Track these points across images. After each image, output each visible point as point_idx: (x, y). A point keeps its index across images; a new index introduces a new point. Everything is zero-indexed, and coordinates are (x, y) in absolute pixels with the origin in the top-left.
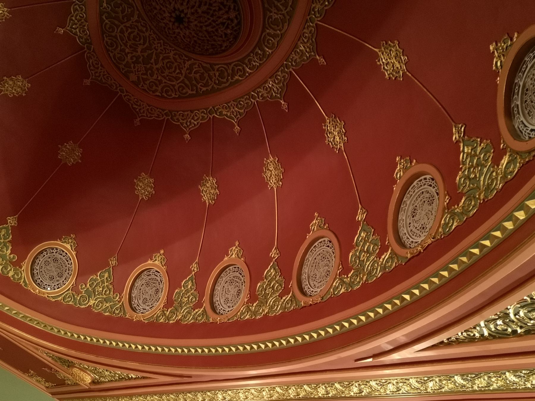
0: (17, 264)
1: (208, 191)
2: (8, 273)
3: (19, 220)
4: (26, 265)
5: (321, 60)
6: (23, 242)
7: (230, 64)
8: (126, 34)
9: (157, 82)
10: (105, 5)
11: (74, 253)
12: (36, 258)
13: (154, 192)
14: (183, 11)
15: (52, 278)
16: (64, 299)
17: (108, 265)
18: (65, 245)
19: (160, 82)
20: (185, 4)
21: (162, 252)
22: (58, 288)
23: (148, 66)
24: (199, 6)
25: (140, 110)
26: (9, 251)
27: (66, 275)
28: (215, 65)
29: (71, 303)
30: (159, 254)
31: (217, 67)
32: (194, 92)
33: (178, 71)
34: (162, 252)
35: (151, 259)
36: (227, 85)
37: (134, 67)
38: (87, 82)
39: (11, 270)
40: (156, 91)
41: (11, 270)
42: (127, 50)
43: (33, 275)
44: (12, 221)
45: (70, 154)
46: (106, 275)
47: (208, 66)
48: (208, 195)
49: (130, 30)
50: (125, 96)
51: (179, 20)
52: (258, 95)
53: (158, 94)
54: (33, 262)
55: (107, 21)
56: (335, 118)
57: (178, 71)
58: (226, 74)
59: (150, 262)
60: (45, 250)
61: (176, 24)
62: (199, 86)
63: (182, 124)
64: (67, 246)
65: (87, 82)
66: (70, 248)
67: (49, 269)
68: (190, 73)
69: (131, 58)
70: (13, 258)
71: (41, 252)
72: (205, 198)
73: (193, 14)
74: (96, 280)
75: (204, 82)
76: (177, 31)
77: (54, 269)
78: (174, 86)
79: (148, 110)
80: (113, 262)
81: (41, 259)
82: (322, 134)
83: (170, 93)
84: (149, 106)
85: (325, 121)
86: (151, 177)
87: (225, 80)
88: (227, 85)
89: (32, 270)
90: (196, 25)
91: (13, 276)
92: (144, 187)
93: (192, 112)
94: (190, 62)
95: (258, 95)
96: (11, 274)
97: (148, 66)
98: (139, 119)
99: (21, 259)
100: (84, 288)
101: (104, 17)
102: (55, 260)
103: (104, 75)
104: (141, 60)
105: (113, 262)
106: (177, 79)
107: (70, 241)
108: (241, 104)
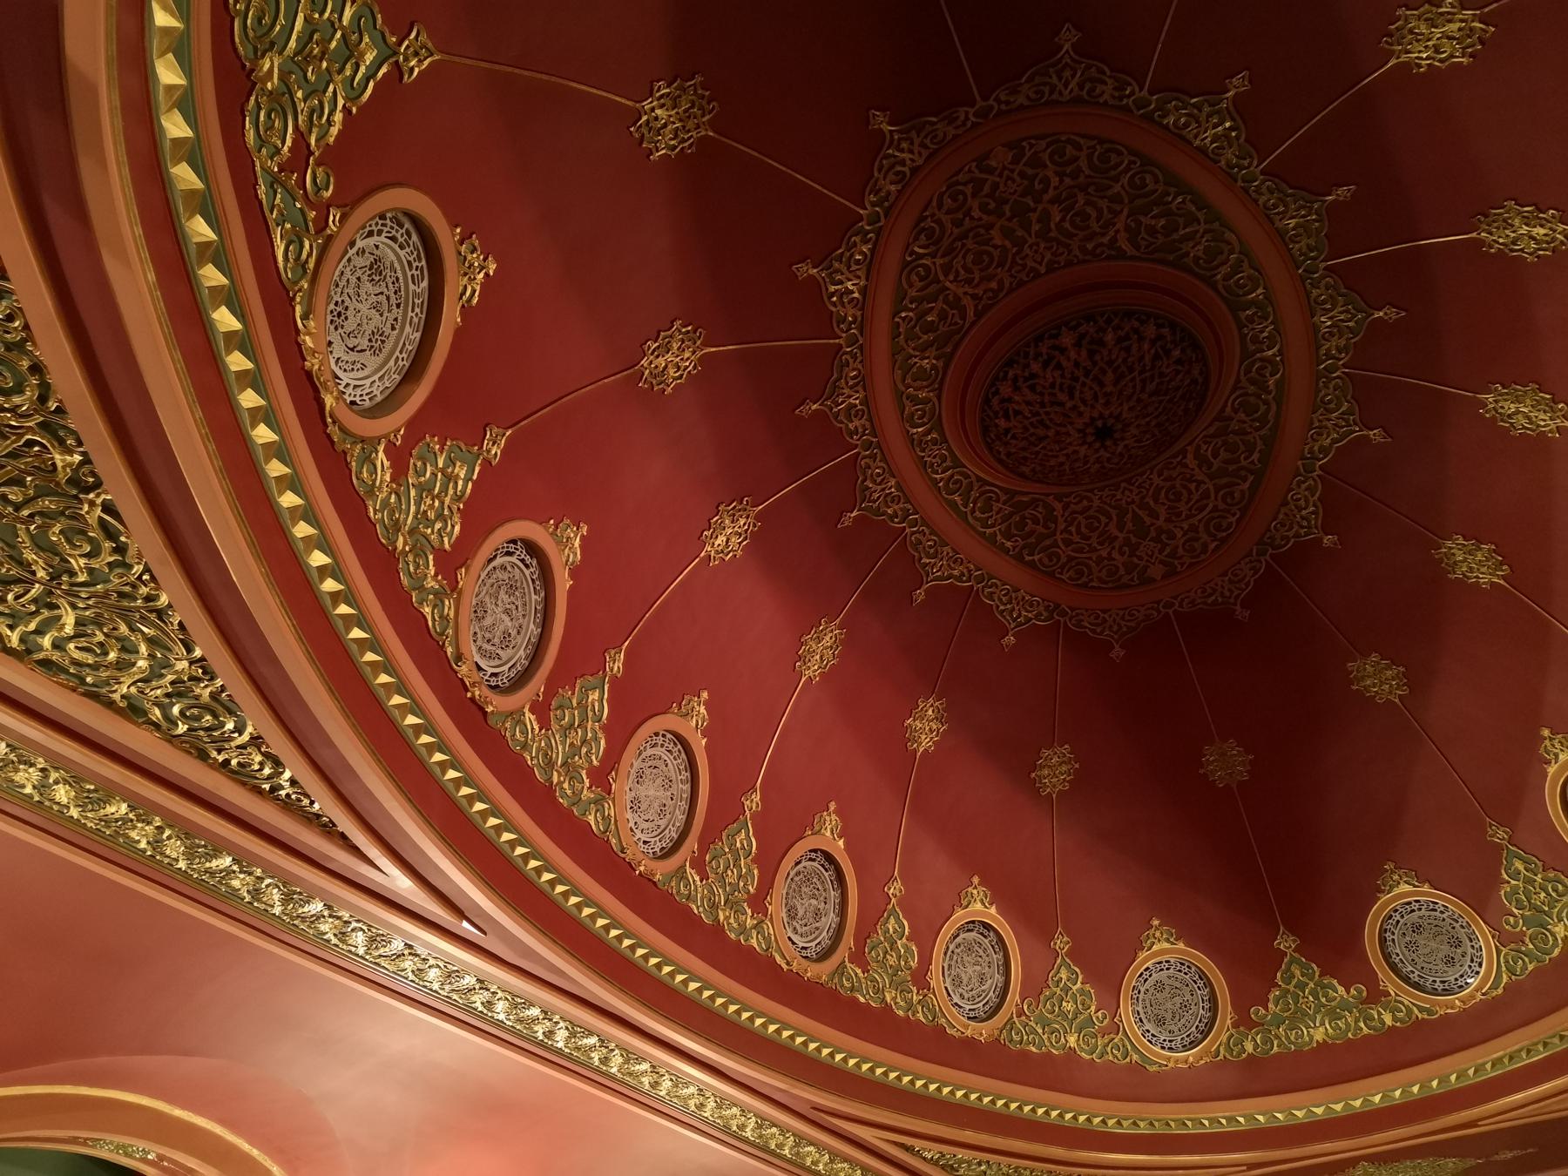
0: (1376, 995)
1: (1475, 565)
2: (1384, 1023)
3: (1292, 930)
4: (1389, 983)
5: (1343, 192)
6: (1338, 952)
7: (1238, 381)
8: (1076, 538)
9: (1190, 535)
10: (1009, 544)
11: (1426, 888)
12: (1387, 957)
13: (1401, 669)
14: (1093, 419)
15: (1450, 961)
16: (1511, 971)
17: (1499, 847)
18: (1396, 891)
19: (1194, 528)
20: (1082, 408)
21: (1546, 733)
22: (1480, 965)
23: (1153, 534)
24: (1102, 385)
25: (1222, 594)
26: (1341, 989)
27: (1462, 934)
28: (1223, 410)
29: (1530, 967)
30: (1547, 742)
31: (1228, 409)
32: (1252, 478)
33: (1193, 486)
34: (1546, 733)
35: (1549, 763)
36: (1274, 407)
37: (1140, 558)
38: (1118, 652)
39: (1379, 1014)
40: (1205, 545)
41: (1379, 1014)
42: (1104, 554)
43: (1416, 986)
44: (1286, 943)
45: (1226, 763)
46: (1519, 865)
47: (1217, 424)
48: (1484, 569)
49: (1073, 529)
50: (1181, 606)
51: (1104, 434)
52: (1333, 357)
53: (1213, 546)
54: (1394, 968)
55: (1036, 558)
56: (1486, 216)
57: (1193, 486)
58: (1252, 399)
59: (1551, 770)
60: (1383, 931)
61: (1108, 443)
62: (1244, 463)
63: (1297, 535)
64: (1403, 890)
65: (1118, 652)
66: (1410, 888)
67: (1427, 951)
68: (1210, 466)
69: (1122, 554)
70: (1360, 992)
71: (1383, 941)
72: (1485, 579)
73: (1107, 404)
74: (1515, 891)
75: (1242, 448)
76: (1119, 449)
77: (1433, 945)
78: (1215, 508)
79: (1231, 581)
80: (1500, 835)
81: (1397, 951)
82: (1507, 263)
83: (1225, 525)
84: (1225, 574)
85: (1482, 242)
86: (1366, 655)
87: (1263, 408)
88: (1274, 407)
89: (1407, 980)
90: (1131, 409)
91: (1395, 1019)
92: (1379, 679)
93: (1285, 504)
94: (1190, 456)
95: (1333, 357)
96: (1388, 1019)
97: (1153, 534)
98: (1238, 607)
99: (1371, 980)
100: (1516, 922)
101: (1028, 558)
102: (1417, 928)
103: (1123, 618)
104: (1134, 540)
105: (1500, 835)
106: (1206, 495)
107: (1396, 877)
108: (1330, 402)
